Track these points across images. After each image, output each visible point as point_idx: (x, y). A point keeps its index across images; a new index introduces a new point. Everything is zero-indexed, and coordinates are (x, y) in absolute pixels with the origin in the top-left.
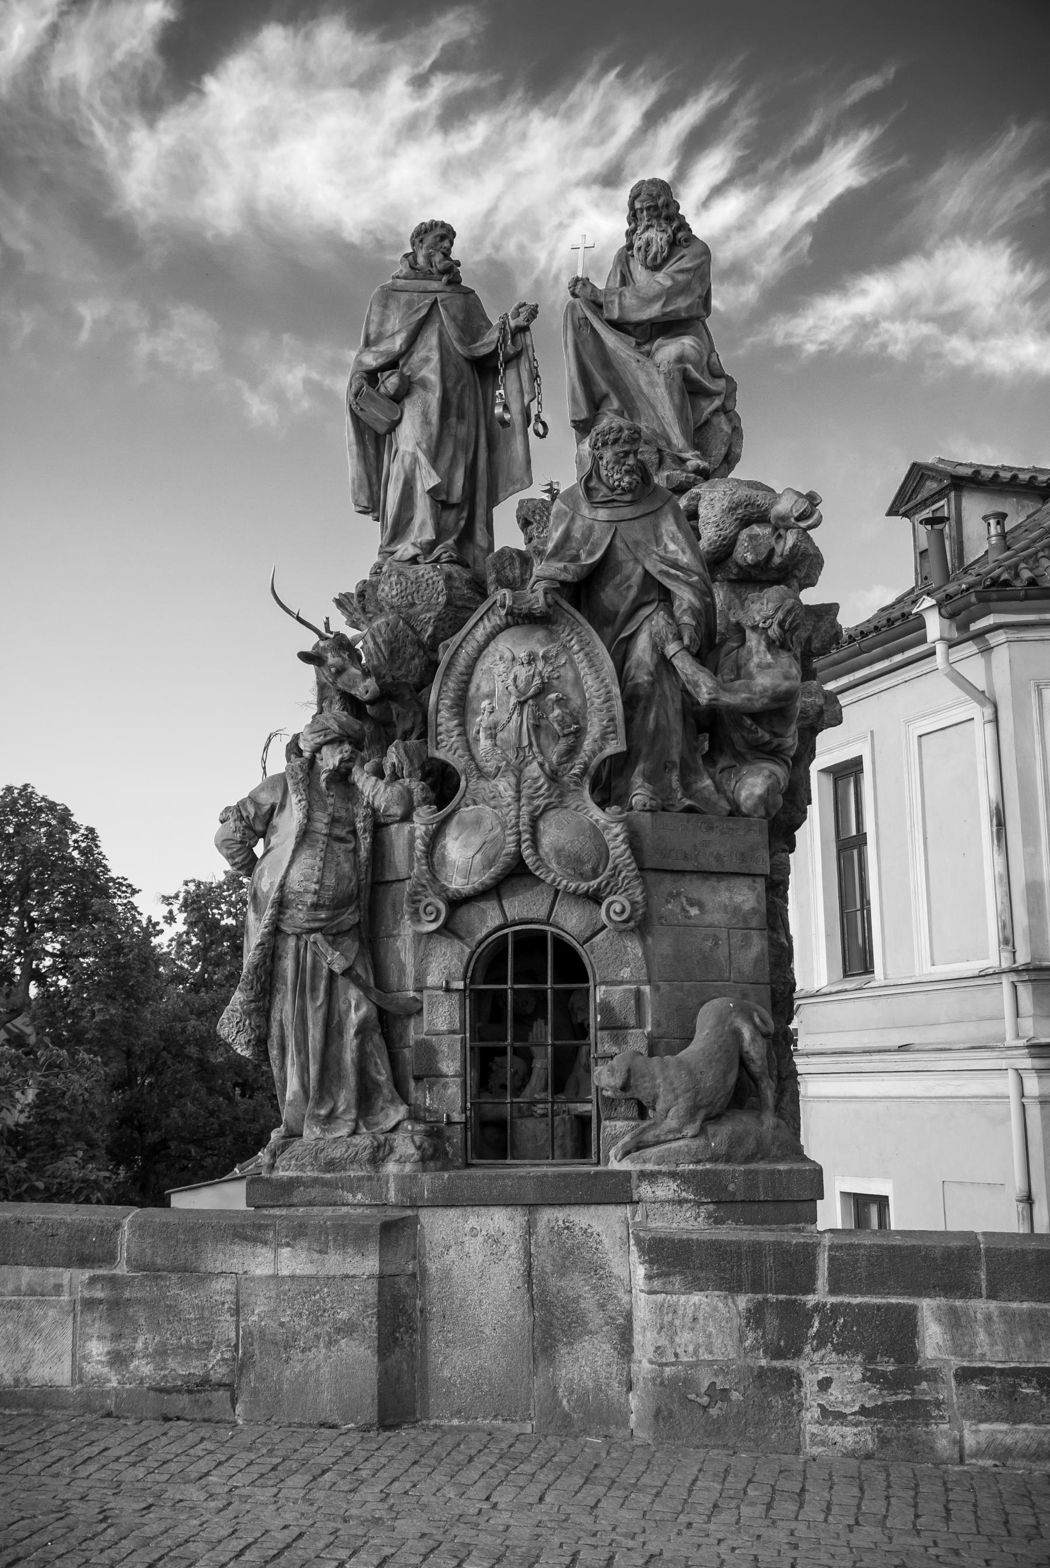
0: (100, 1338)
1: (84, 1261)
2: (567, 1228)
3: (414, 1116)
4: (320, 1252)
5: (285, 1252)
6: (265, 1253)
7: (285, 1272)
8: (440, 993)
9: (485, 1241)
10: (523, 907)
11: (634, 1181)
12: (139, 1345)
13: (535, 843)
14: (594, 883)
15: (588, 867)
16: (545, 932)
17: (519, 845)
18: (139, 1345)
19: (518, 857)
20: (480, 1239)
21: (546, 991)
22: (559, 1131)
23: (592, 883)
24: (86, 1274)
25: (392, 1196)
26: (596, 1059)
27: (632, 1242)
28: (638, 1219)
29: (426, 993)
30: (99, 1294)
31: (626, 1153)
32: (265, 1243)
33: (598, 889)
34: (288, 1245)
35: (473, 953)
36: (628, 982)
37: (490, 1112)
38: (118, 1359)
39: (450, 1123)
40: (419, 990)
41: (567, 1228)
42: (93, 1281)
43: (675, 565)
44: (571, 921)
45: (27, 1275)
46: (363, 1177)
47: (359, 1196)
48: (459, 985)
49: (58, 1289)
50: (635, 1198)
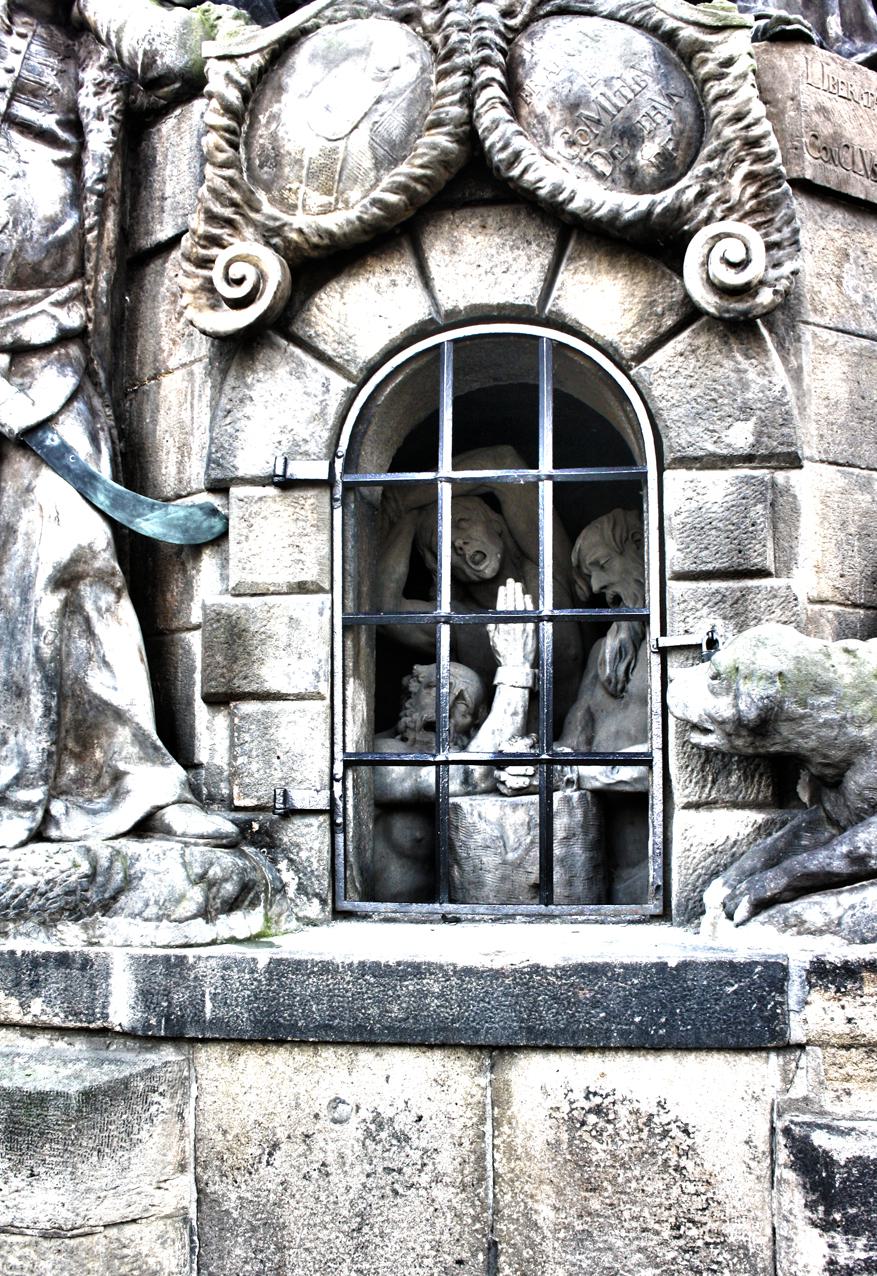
2: (598, 1110)
3: (200, 795)
8: (271, 491)
9: (369, 1134)
11: (795, 990)
13: (513, 90)
14: (666, 197)
15: (647, 154)
16: (537, 338)
17: (468, 98)
19: (470, 137)
20: (352, 1132)
21: (533, 487)
22: (560, 825)
23: (658, 197)
25: (122, 1011)
26: (664, 653)
27: (783, 1155)
28: (798, 1091)
29: (235, 491)
31: (760, 906)
33: (677, 213)
35: (352, 396)
36: (748, 459)
37: (401, 779)
39: (291, 813)
40: (220, 487)
41: (598, 1110)
46: (47, 956)
47: (37, 1005)
50: (796, 1034)
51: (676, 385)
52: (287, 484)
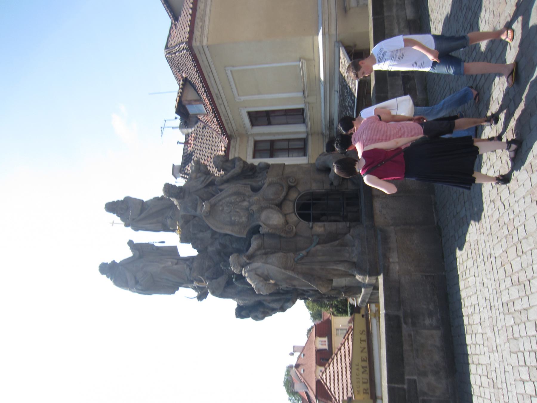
0: (424, 320)
1: (399, 327)
4: (390, 249)
5: (391, 260)
6: (392, 266)
7: (397, 260)
10: (289, 207)
12: (425, 307)
18: (425, 307)
24: (404, 326)
30: (410, 320)
32: (389, 266)
34: (389, 259)
38: (431, 315)
42: (406, 323)
43: (203, 181)
44: (294, 195)
45: (406, 347)
48: (311, 223)
49: (410, 335)
51: (302, 188)
52: (312, 228)
